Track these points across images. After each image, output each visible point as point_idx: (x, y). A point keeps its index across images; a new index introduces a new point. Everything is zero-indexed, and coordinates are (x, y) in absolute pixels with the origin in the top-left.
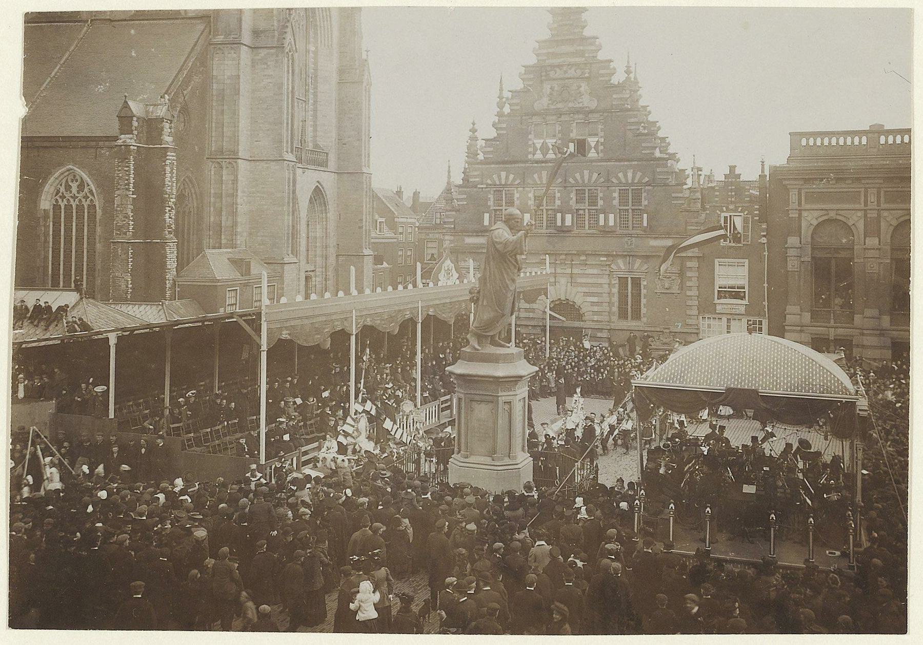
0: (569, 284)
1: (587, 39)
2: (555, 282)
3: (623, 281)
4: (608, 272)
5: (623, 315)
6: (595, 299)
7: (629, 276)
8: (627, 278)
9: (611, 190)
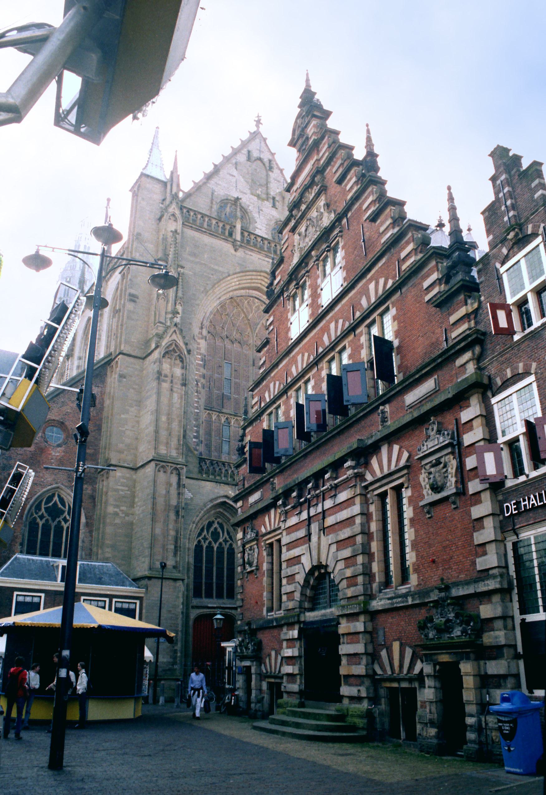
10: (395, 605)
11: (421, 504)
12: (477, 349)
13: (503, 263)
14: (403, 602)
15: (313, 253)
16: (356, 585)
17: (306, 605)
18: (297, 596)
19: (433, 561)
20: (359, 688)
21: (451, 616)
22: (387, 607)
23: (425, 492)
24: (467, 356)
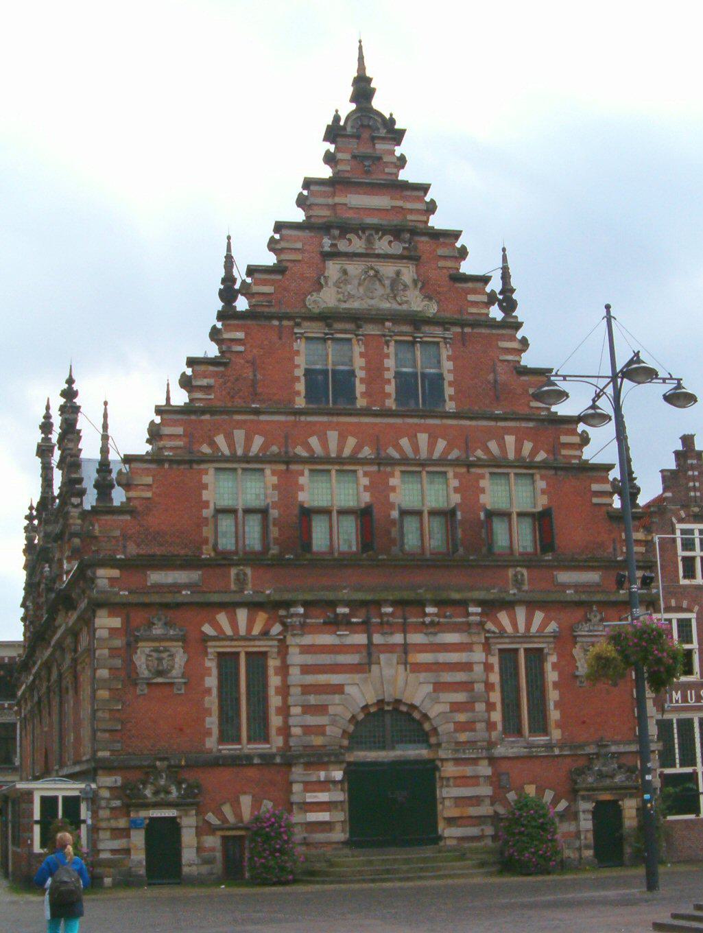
0: (401, 668)
1: (406, 186)
3: (508, 657)
4: (483, 641)
5: (512, 726)
6: (460, 697)
7: (522, 647)
8: (516, 651)
10: (534, 754)
11: (577, 673)
15: (388, 324)
16: (474, 730)
18: (334, 731)
19: (584, 722)
20: (483, 827)
21: (616, 766)
23: (578, 664)
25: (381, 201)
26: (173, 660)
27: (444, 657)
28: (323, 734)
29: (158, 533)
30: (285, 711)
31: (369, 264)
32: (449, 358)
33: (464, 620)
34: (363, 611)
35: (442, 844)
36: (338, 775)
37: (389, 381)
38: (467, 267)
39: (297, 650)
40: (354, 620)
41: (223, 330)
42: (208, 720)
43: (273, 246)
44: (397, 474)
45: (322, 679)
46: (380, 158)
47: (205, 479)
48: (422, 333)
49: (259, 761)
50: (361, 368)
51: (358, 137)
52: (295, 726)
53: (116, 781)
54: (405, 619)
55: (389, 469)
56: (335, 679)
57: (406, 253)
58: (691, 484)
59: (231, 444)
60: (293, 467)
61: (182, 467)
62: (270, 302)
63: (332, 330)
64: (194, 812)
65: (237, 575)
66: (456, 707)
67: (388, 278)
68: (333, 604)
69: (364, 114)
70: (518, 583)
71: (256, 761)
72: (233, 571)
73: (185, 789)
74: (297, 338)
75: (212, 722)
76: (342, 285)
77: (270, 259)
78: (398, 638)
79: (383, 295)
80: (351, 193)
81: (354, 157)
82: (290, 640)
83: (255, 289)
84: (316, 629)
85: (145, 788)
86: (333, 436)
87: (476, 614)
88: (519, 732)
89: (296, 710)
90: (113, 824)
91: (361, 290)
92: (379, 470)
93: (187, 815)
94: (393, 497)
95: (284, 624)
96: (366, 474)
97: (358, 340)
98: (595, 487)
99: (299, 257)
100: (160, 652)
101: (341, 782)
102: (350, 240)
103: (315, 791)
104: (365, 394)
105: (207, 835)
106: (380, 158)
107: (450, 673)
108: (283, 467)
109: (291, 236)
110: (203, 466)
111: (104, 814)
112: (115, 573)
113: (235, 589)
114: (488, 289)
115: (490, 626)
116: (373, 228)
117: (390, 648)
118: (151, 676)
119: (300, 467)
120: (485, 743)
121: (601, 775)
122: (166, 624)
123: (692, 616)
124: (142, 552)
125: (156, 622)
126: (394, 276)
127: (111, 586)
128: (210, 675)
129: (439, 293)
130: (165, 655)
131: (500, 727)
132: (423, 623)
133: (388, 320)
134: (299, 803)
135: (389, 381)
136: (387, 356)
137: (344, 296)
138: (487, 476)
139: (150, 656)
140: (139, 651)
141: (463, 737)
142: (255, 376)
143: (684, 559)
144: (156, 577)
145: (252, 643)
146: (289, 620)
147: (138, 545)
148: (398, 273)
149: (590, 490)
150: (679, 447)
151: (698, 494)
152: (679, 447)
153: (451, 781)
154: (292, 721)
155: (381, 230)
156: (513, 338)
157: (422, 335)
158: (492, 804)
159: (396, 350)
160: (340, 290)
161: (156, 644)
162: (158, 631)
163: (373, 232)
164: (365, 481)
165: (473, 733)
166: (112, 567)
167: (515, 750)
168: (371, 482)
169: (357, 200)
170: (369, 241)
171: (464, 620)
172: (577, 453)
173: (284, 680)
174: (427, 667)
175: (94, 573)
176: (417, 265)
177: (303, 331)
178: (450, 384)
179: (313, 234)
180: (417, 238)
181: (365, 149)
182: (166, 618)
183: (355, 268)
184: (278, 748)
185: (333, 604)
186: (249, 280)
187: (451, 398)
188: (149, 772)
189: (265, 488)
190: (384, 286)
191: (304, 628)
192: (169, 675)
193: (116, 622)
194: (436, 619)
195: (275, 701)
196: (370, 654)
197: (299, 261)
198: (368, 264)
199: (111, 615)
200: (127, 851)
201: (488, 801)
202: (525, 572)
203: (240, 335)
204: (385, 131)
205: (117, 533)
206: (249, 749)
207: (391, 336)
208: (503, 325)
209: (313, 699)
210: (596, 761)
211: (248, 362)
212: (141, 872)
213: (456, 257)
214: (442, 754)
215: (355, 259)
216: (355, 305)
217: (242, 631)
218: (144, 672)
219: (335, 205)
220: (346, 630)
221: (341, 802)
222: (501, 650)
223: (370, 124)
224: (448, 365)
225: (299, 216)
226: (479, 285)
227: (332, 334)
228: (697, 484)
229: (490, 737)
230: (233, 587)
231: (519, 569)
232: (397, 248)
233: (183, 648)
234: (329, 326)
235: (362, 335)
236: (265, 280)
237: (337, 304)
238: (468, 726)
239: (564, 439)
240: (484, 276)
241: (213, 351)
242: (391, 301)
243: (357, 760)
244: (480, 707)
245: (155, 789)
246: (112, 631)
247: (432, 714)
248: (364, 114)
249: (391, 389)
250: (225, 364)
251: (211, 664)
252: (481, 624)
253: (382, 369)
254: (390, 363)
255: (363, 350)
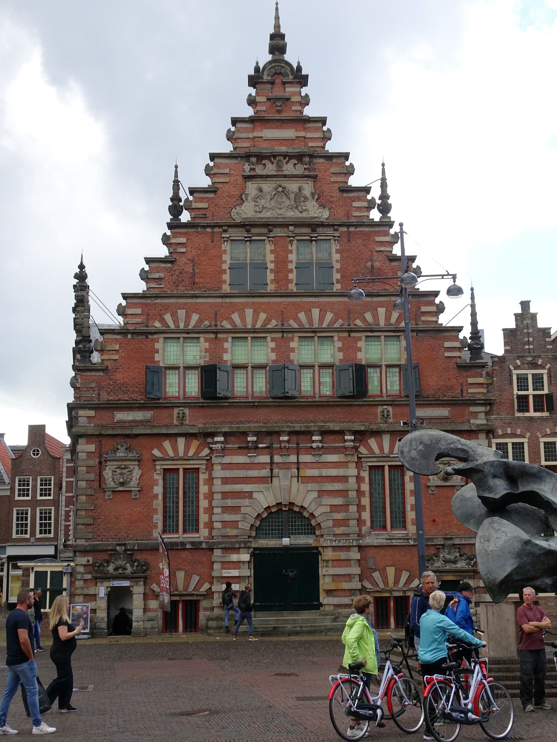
2: (272, 477)
6: (338, 501)
8: (383, 467)
9: (354, 337)
10: (395, 544)
11: (428, 484)
12: (488, 407)
13: (515, 369)
14: (404, 543)
15: (291, 228)
16: (348, 526)
17: (254, 534)
18: (245, 526)
19: (434, 521)
22: (384, 544)
24: (482, 409)
25: (289, 133)
26: (132, 474)
27: (326, 472)
28: (237, 528)
29: (123, 385)
30: (210, 510)
31: (278, 183)
32: (337, 251)
33: (341, 445)
34: (268, 439)
35: (321, 609)
36: (245, 557)
37: (291, 271)
38: (354, 181)
39: (219, 467)
40: (260, 446)
41: (171, 237)
42: (155, 517)
43: (208, 172)
44: (296, 339)
45: (237, 487)
46: (288, 99)
47: (157, 346)
48: (317, 233)
49: (190, 547)
50: (271, 262)
51: (272, 83)
52: (216, 521)
53: (88, 561)
54: (298, 444)
55: (290, 335)
56: (247, 488)
57: (307, 173)
58: (526, 339)
59: (176, 321)
60: (220, 336)
61: (140, 337)
62: (205, 215)
63: (251, 234)
64: (142, 583)
65: (178, 413)
66: (334, 508)
67: (293, 192)
68: (245, 434)
69: (277, 64)
70: (385, 417)
71: (188, 546)
72: (176, 411)
73: (137, 566)
74: (224, 241)
75: (158, 518)
76: (258, 200)
77: (205, 182)
78: (293, 458)
79: (288, 206)
80: (266, 128)
81: (269, 99)
82: (215, 460)
83: (194, 205)
84: (232, 452)
85: (108, 566)
86: (249, 312)
87: (351, 441)
88: (384, 528)
89: (217, 510)
90: (86, 591)
91: (273, 202)
92: (283, 336)
93: (137, 585)
94: (292, 356)
95: (211, 449)
96: (273, 340)
97: (269, 241)
98: (447, 344)
99: (227, 180)
100: (122, 469)
101: (249, 562)
102: (264, 164)
103: (229, 569)
104: (274, 281)
105: (151, 599)
106: (288, 99)
107: (331, 484)
108: (213, 336)
109: (221, 164)
110: (155, 336)
111: (79, 584)
112: (92, 413)
113: (176, 424)
114: (369, 197)
115: (362, 450)
116: (281, 155)
117: (286, 466)
118: (115, 486)
119: (225, 336)
120: (356, 535)
121: (446, 561)
122: (126, 449)
123: (525, 440)
124: (111, 398)
125: (119, 448)
126: (298, 191)
127: (90, 423)
128: (157, 485)
129: (331, 202)
130: (125, 471)
131: (368, 523)
132: (311, 447)
133: (291, 225)
134: (218, 577)
135: (291, 271)
136: (291, 252)
137: (259, 208)
138: (364, 338)
139: (116, 472)
140: (107, 468)
141: (339, 531)
142: (194, 270)
143: (519, 397)
144: (120, 416)
145: (187, 462)
146: (214, 446)
147: (108, 393)
148: (300, 189)
149: (443, 347)
150: (519, 311)
151: (531, 347)
152: (519, 311)
153: (330, 562)
154: (214, 518)
155: (288, 156)
156: (387, 234)
157: (316, 235)
158: (361, 581)
159: (297, 247)
160: (256, 203)
161: (120, 463)
162: (121, 454)
163: (282, 158)
164: (273, 345)
165: (347, 528)
166: (90, 409)
167: (379, 541)
168: (276, 345)
169: (269, 133)
170: (279, 167)
171: (341, 445)
172: (434, 319)
173: (210, 489)
174: (312, 479)
175: (77, 413)
176: (314, 182)
177: (228, 236)
178: (338, 271)
179: (237, 161)
180: (315, 160)
181: (278, 92)
182: (127, 444)
183: (268, 187)
184: (204, 538)
185: (245, 434)
186: (191, 198)
187: (338, 281)
188: (113, 554)
189: (201, 351)
190: (289, 199)
191: (224, 451)
192: (128, 485)
193: (92, 448)
194: (320, 445)
195: (203, 503)
196: (272, 470)
197: (227, 182)
198: (277, 182)
199: (87, 443)
200: (94, 611)
201: (357, 578)
202: (390, 409)
203: (183, 240)
204: (292, 77)
205: (94, 385)
206: (184, 538)
207: (294, 237)
208: (380, 224)
209: (230, 502)
210: (441, 550)
211: (189, 260)
212: (103, 626)
213: (345, 174)
214: (323, 542)
215: (268, 179)
216: (267, 214)
217: (181, 454)
218: (110, 483)
219: (254, 138)
220: (255, 453)
221: (249, 576)
222: (370, 466)
223: (282, 72)
224: (336, 257)
225: (227, 147)
226: (362, 194)
227: (250, 237)
228: (531, 339)
229: (360, 530)
230: (175, 422)
231: (385, 407)
232: (300, 170)
233: (138, 465)
234: (248, 231)
235: (273, 237)
236: (202, 198)
237: (254, 214)
238: (344, 522)
239: (424, 309)
240: (365, 187)
241: (163, 252)
242: (295, 210)
243: (260, 546)
244: (353, 509)
245: (115, 566)
246: (89, 453)
247: (316, 514)
248: (277, 64)
249: (292, 276)
250: (172, 262)
251: (159, 478)
252: (356, 448)
253: (286, 261)
254: (292, 257)
255: (273, 248)
